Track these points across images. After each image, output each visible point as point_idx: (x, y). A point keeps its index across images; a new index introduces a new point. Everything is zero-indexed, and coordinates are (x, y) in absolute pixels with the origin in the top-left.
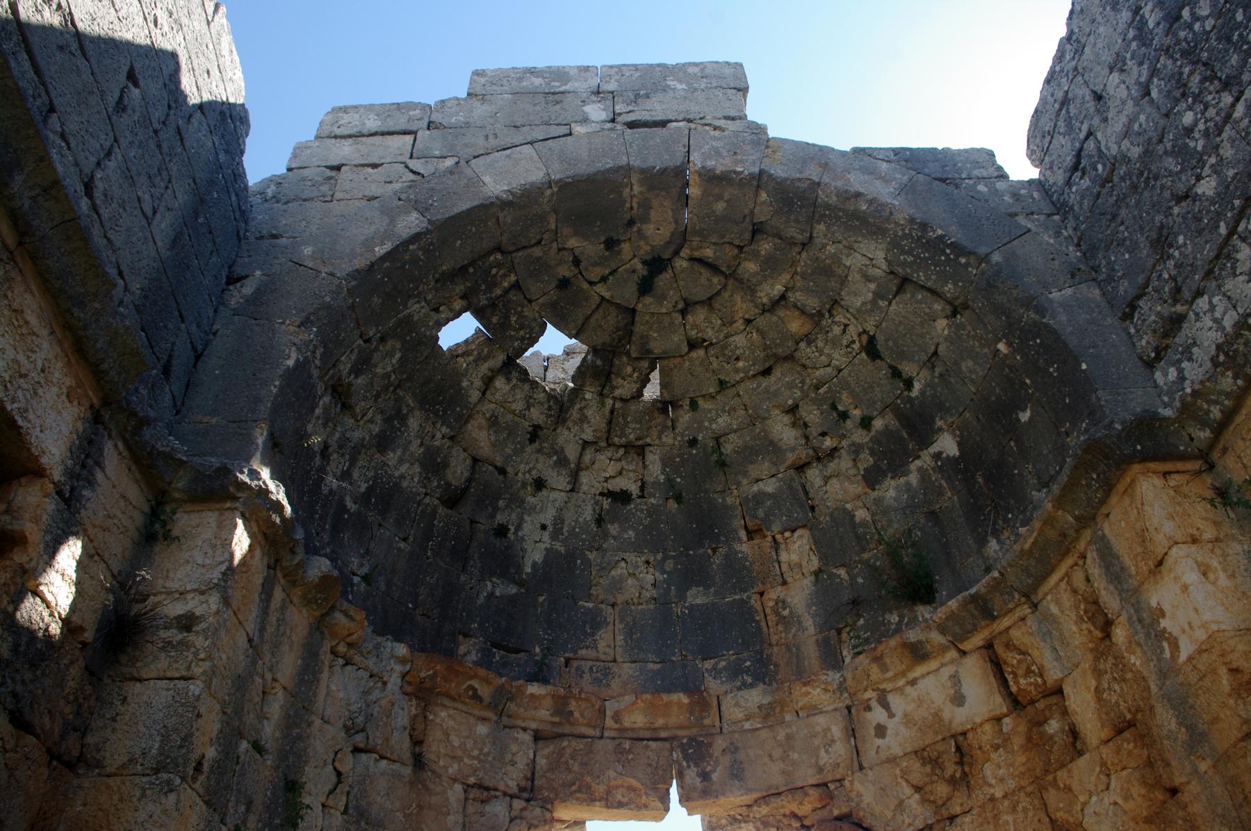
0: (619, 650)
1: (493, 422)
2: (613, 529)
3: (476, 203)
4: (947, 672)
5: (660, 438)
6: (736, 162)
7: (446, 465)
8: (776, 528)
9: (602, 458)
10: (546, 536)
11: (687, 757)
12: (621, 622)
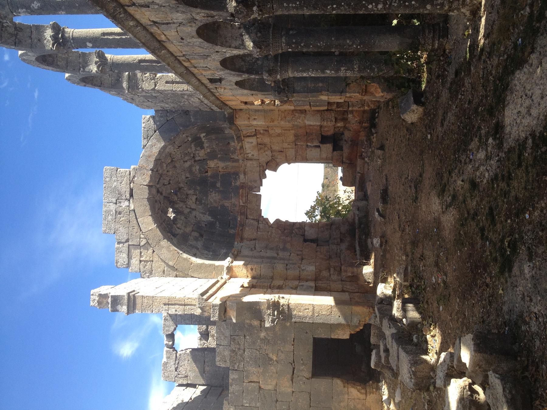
1: (185, 227)
2: (203, 201)
4: (246, 143)
8: (206, 167)
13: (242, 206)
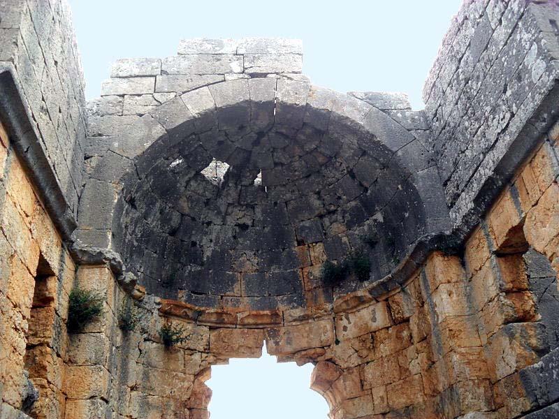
0: (243, 292)
1: (189, 199)
2: (241, 240)
3: (185, 120)
4: (371, 308)
7: (170, 219)
9: (236, 210)
11: (269, 336)
12: (244, 279)
13: (236, 317)
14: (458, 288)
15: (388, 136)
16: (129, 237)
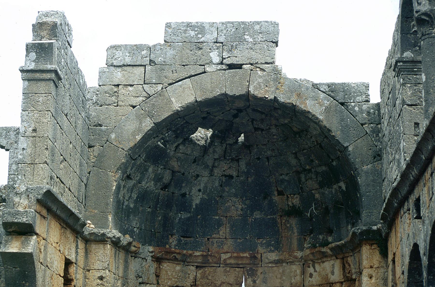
2: (227, 189)
3: (170, 114)
4: (332, 262)
5: (245, 157)
6: (266, 91)
7: (162, 178)
10: (201, 193)
12: (228, 224)
13: (220, 258)
14: (378, 273)
15: (342, 131)
16: (126, 203)
